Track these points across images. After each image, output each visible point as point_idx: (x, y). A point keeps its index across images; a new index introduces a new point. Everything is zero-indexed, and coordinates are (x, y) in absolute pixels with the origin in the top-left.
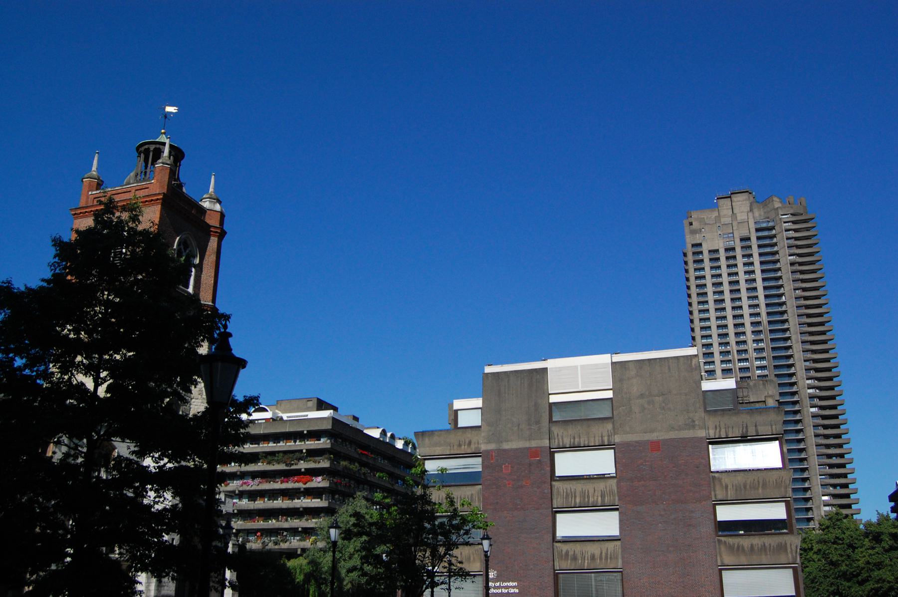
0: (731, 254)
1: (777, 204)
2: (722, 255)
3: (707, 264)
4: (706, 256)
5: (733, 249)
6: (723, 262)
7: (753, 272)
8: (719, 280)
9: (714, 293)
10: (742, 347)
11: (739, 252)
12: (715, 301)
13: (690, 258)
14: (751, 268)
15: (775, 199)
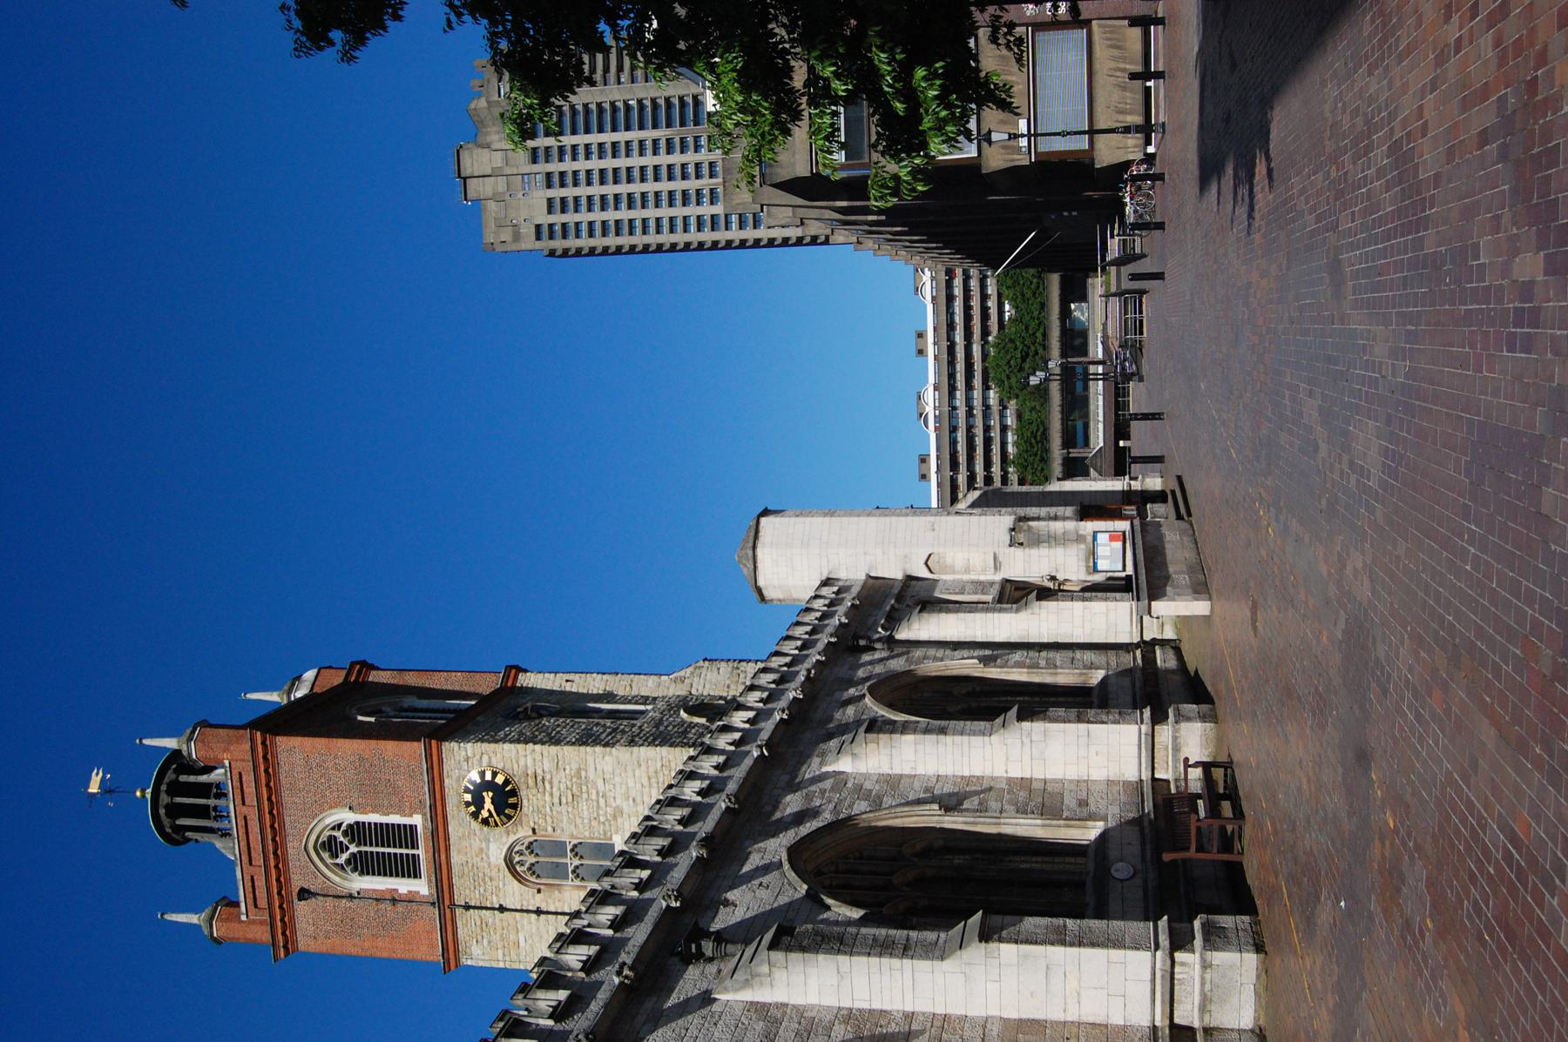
0: (556, 179)
1: (483, 103)
2: (557, 193)
3: (570, 218)
4: (558, 219)
5: (549, 175)
6: (569, 192)
7: (587, 146)
8: (597, 200)
9: (616, 208)
10: (705, 170)
11: (555, 167)
12: (630, 207)
13: (558, 244)
14: (581, 150)
15: (472, 106)
